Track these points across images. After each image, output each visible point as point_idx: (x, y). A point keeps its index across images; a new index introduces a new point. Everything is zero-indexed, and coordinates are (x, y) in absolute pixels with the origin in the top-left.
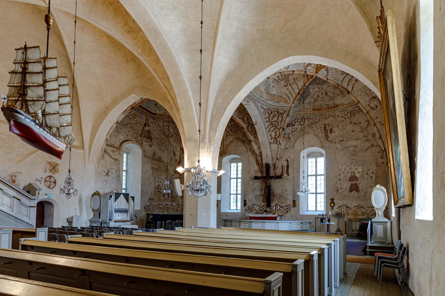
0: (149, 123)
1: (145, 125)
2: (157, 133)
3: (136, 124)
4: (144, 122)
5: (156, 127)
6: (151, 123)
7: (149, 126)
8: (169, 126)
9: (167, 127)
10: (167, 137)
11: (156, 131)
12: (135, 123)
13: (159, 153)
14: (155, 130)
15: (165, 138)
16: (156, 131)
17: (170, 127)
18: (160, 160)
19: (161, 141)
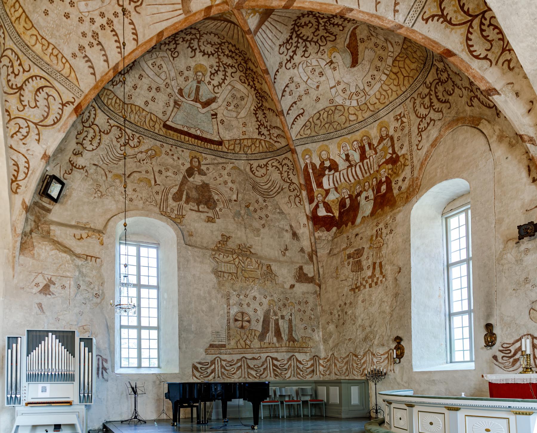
0: (203, 168)
1: (190, 172)
2: (231, 189)
3: (160, 172)
4: (188, 165)
5: (229, 174)
6: (211, 167)
7: (202, 173)
8: (266, 165)
9: (263, 171)
10: (266, 195)
11: (230, 185)
12: (156, 169)
13: (240, 236)
14: (226, 183)
15: (261, 199)
16: (230, 185)
17: (270, 168)
18: (244, 251)
19: (248, 207)
